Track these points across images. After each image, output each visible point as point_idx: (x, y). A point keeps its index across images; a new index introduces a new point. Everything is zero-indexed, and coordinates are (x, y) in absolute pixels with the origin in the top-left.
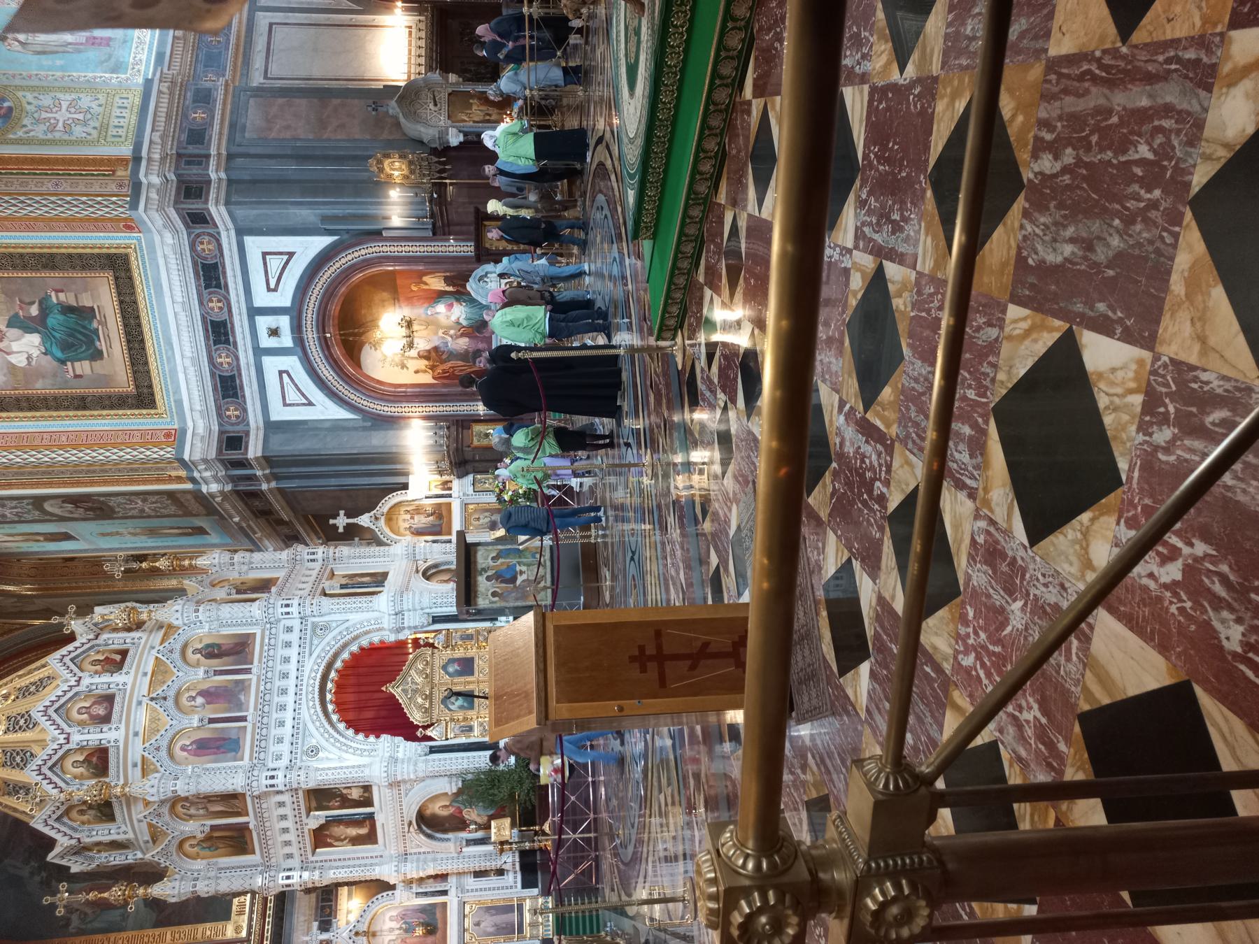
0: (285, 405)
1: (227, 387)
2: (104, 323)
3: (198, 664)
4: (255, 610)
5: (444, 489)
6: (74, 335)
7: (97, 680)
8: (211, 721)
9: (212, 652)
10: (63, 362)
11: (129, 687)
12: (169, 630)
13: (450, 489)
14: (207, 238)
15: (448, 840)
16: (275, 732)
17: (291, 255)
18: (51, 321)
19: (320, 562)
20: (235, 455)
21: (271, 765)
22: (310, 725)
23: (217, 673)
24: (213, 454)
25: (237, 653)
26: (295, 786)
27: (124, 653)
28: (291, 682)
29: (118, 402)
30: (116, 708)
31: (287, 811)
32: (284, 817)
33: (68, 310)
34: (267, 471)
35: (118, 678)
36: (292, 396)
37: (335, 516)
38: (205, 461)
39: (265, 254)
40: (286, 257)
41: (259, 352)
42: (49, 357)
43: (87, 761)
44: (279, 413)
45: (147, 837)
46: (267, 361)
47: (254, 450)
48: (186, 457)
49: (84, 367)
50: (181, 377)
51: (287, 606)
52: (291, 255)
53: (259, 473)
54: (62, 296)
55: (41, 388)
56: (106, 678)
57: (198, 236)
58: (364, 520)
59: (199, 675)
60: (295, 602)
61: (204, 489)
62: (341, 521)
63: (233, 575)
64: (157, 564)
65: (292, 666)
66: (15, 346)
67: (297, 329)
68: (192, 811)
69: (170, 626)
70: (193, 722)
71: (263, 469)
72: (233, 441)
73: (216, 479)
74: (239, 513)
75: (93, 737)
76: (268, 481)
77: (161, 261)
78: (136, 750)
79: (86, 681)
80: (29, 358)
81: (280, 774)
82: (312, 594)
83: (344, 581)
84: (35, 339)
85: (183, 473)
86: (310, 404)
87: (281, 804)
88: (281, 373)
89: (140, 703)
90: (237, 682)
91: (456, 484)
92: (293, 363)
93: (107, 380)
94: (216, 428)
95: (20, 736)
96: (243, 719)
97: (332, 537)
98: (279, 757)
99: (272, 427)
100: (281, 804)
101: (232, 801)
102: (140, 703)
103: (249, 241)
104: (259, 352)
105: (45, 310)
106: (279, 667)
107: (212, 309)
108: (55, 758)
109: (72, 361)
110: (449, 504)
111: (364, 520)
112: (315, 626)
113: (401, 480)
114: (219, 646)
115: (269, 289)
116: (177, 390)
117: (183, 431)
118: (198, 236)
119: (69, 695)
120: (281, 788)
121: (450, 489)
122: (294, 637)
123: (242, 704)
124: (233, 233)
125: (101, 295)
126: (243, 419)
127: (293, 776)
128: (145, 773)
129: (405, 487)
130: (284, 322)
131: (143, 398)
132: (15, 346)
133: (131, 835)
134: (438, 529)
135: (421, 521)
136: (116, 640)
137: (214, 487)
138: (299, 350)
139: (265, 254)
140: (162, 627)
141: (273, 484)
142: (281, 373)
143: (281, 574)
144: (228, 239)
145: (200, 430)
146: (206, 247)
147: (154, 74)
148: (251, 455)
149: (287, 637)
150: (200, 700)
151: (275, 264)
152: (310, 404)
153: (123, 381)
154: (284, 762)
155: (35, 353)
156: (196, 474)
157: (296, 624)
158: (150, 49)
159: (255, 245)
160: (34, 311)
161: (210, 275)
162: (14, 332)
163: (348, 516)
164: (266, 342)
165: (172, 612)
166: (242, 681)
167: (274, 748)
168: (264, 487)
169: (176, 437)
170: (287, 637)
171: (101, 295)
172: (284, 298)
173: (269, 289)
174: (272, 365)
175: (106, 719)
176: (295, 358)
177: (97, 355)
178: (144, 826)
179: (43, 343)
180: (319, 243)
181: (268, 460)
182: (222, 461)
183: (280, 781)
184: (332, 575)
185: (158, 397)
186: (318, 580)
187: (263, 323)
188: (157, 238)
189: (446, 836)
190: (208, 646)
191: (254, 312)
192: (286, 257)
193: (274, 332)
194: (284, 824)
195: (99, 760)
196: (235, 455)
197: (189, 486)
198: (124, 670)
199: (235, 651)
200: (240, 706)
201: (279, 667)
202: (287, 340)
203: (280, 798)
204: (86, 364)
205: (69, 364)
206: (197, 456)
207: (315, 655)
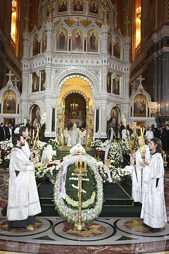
3: (88, 34)
5: (151, 114)
9: (93, 39)
13: (151, 116)
15: (30, 114)
21: (53, 59)
25: (91, 47)
59: (85, 36)
90: (82, 47)
91: (154, 118)
96: (70, 50)
110: (145, 116)
111: (141, 87)
113: (155, 99)
114: (94, 41)
121: (151, 116)
123: (75, 49)
129: (153, 101)
134: (136, 112)
135: (139, 106)
143: (121, 59)
150: (77, 36)
166: (82, 49)
167: (59, 60)
189: (31, 114)
190: (95, 37)
200: (74, 48)
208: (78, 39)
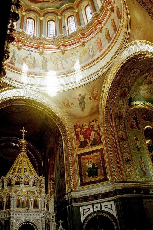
0: (83, 210)
1: (85, 199)
2: (95, 177)
4: (43, 209)
6: (93, 172)
7: (32, 182)
8: (23, 202)
9: (35, 201)
10: (88, 171)
11: (30, 187)
12: (40, 193)
14: (112, 194)
16: (20, 214)
17: (112, 210)
18: (94, 169)
19: (52, 219)
20: (73, 201)
22: (21, 220)
23: (31, 202)
24: (73, 197)
26: (10, 218)
27: (36, 185)
28: (29, 216)
29: (81, 181)
30: (26, 185)
31: (6, 217)
32: (4, 216)
33: (97, 171)
34: (70, 207)
35: (32, 185)
36: (85, 211)
37: (61, 221)
38: (71, 196)
39: (111, 205)
40: (111, 209)
41: (93, 204)
42: (88, 169)
43: (18, 182)
44: (81, 209)
45: (4, 192)
46: (92, 206)
47: (74, 204)
48: (72, 193)
49: (87, 174)
50: (87, 191)
51: (43, 214)
52: (112, 210)
53: (70, 205)
54: (99, 171)
55: (83, 168)
56: (32, 183)
57: (113, 193)
58: (61, 227)
59: (31, 199)
60: (44, 216)
61: (66, 195)
62: (61, 222)
63: (49, 203)
64: (52, 189)
65: (32, 216)
66: (90, 164)
67: (98, 211)
68: (7, 200)
69: (40, 193)
70: (23, 199)
71: (70, 206)
72: (76, 200)
73: (68, 198)
74: (62, 201)
75: (22, 182)
76: (68, 207)
77: (107, 187)
78: (19, 190)
79: (31, 180)
80: (88, 166)
81: (12, 216)
82: (46, 218)
83: (48, 224)
84: (91, 167)
85: (69, 191)
86: (84, 215)
87: (7, 216)
88: (89, 209)
89: (27, 189)
92: (91, 211)
93: (85, 178)
94: (78, 197)
95: (23, 170)
97: (57, 220)
98: (15, 215)
99: (79, 207)
100: (7, 216)
101: (8, 207)
102: (27, 189)
103: (113, 202)
104: (93, 204)
105: (97, 168)
106: (32, 214)
107: (100, 196)
108: (19, 177)
109: (88, 173)
111: (61, 227)
112: (39, 220)
114: (36, 202)
115: (105, 206)
116: (84, 190)
117: (77, 191)
118: (113, 193)
119: (29, 178)
120: (10, 216)
122: (38, 216)
124: (114, 199)
125: (99, 177)
126: (80, 202)
127: (12, 218)
128: (15, 191)
130: (99, 209)
131: (82, 184)
132: (90, 164)
133: (4, 189)
136: (38, 184)
137: (67, 197)
138: (94, 212)
139: (111, 205)
140: (40, 191)
141: (68, 208)
142: (89, 209)
144: (113, 198)
145: (77, 195)
146: (111, 194)
147: (141, 183)
148: (73, 204)
149: (38, 215)
150: (27, 200)
151: (110, 207)
152: (84, 215)
153: (86, 181)
154: (15, 216)
155: (89, 167)
156: (69, 194)
157: (40, 216)
158: (146, 182)
159: (113, 203)
160: (96, 167)
161: (106, 195)
162: (92, 164)
163: (62, 223)
164: (95, 206)
165: (43, 194)
167: (17, 214)
168: (67, 206)
169: (76, 191)
170: (38, 215)
171: (99, 177)
172: (104, 209)
173: (105, 206)
174: (91, 207)
175: (25, 184)
176: (92, 211)
177: (89, 176)
178: (6, 191)
179: (91, 168)
180: (115, 215)
181: (72, 206)
182: (72, 198)
183: (11, 216)
184: (49, 221)
185: (83, 187)
186: (48, 219)
187: (98, 205)
188: (111, 186)
190: (36, 200)
191: (100, 203)
192: (111, 209)
193: (97, 207)
194: (3, 216)
195: (18, 183)
196: (73, 201)
197: (67, 193)
198: (33, 186)
199: (36, 206)
201: (32, 214)
202: (96, 210)
203: (8, 215)
204: (88, 175)
205: (87, 172)
206: (72, 194)
207: (34, 220)
208: (27, 202)
